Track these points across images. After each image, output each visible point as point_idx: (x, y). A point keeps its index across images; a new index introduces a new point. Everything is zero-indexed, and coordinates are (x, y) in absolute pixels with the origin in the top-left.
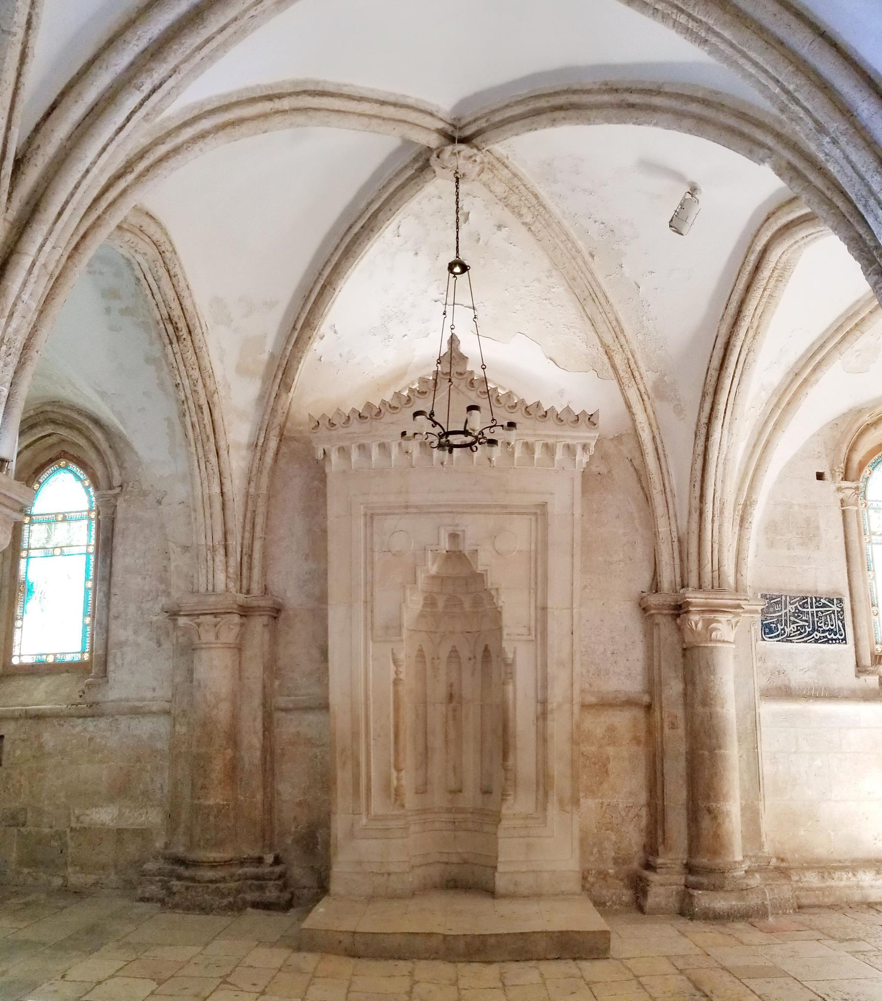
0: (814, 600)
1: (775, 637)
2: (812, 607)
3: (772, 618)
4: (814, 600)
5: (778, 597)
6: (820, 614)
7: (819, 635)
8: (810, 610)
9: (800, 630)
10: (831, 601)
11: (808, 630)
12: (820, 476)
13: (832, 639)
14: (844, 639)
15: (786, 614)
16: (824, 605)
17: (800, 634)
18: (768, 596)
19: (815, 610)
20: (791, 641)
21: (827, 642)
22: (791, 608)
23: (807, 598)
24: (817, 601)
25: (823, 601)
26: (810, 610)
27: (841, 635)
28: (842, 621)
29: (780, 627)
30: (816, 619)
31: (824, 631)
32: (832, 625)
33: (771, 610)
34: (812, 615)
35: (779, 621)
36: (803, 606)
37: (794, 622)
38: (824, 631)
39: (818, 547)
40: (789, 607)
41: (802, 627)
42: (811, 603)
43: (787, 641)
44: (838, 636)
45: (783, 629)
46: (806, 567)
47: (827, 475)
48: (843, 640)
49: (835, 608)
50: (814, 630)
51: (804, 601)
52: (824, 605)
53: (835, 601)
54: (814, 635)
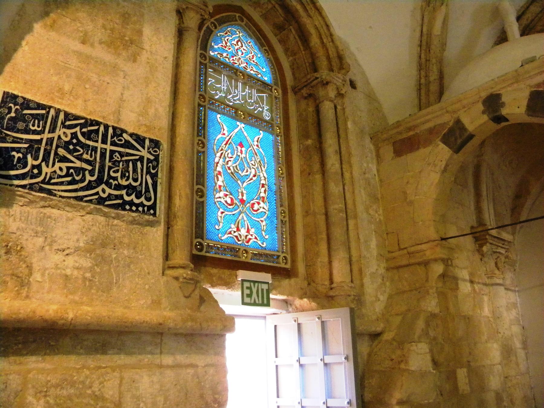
0: (111, 131)
1: (17, 177)
2: (104, 142)
3: (16, 140)
4: (111, 131)
5: (40, 106)
6: (117, 157)
7: (108, 191)
8: (99, 145)
9: (73, 176)
10: (140, 140)
11: (88, 178)
13: (131, 203)
14: (153, 207)
15: (50, 141)
17: (69, 183)
18: (20, 101)
19: (109, 147)
20: (50, 192)
21: (121, 206)
22: (63, 134)
23: (98, 123)
24: (114, 135)
25: (125, 135)
26: (99, 145)
27: (148, 199)
28: (154, 177)
29: (30, 161)
30: (108, 164)
31: (118, 187)
32: (135, 180)
33: (21, 125)
34: (103, 155)
35: (33, 148)
36: (88, 135)
37: (63, 159)
38: (118, 187)
39: (134, 58)
40: (60, 131)
41: (78, 170)
42: (105, 136)
43: (41, 190)
44: (143, 199)
45: (39, 167)
46: (107, 79)
48: (149, 208)
49: (144, 153)
50: (100, 181)
53: (147, 142)
54: (99, 189)
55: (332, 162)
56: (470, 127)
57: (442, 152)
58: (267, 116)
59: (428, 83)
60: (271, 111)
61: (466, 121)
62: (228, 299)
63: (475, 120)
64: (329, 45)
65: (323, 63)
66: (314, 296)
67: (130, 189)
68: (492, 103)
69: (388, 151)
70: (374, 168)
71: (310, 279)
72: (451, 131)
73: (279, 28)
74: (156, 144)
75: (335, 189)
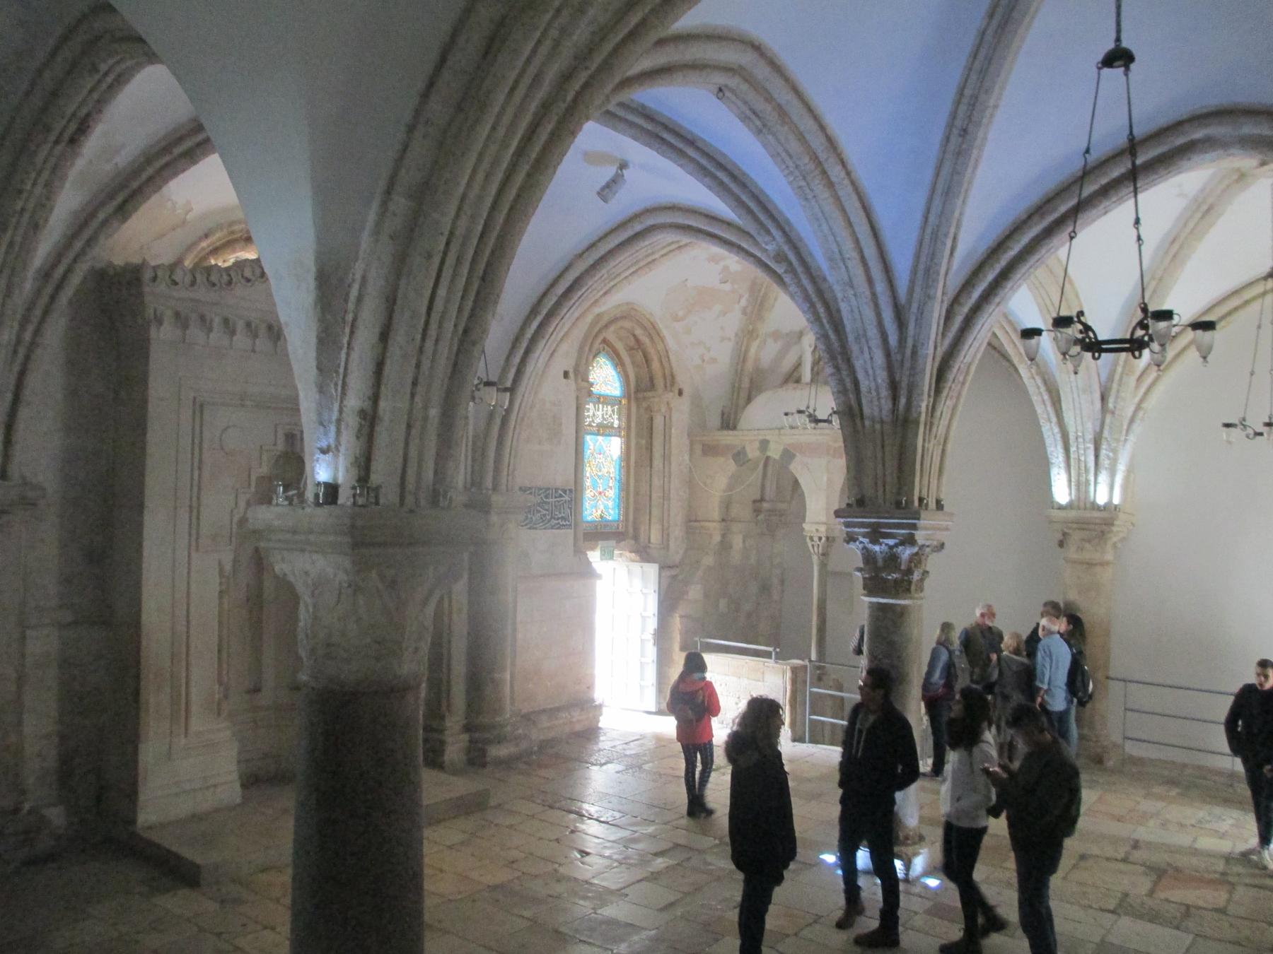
10: (565, 491)
12: (566, 375)
16: (561, 496)
36: (546, 497)
47: (571, 375)
49: (567, 498)
51: (547, 491)
52: (561, 496)
55: (657, 462)
56: (750, 455)
57: (731, 466)
58: (616, 424)
59: (739, 388)
60: (619, 419)
61: (748, 449)
62: (594, 556)
63: (753, 452)
64: (666, 365)
65: (659, 382)
66: (636, 552)
67: (563, 518)
68: (764, 444)
69: (698, 449)
70: (687, 457)
71: (636, 537)
72: (739, 453)
73: (630, 349)
74: (571, 491)
75: (657, 482)
